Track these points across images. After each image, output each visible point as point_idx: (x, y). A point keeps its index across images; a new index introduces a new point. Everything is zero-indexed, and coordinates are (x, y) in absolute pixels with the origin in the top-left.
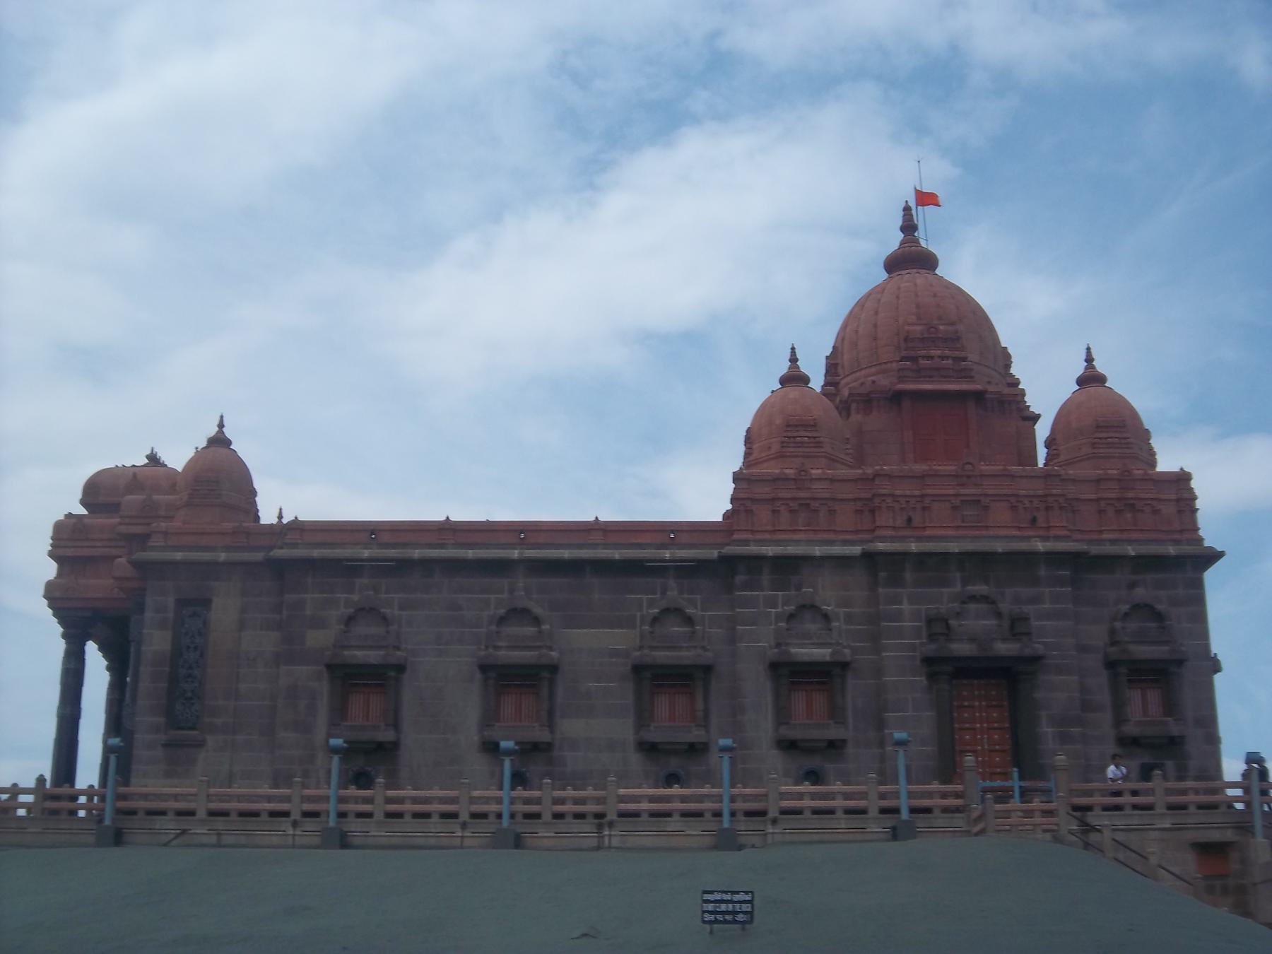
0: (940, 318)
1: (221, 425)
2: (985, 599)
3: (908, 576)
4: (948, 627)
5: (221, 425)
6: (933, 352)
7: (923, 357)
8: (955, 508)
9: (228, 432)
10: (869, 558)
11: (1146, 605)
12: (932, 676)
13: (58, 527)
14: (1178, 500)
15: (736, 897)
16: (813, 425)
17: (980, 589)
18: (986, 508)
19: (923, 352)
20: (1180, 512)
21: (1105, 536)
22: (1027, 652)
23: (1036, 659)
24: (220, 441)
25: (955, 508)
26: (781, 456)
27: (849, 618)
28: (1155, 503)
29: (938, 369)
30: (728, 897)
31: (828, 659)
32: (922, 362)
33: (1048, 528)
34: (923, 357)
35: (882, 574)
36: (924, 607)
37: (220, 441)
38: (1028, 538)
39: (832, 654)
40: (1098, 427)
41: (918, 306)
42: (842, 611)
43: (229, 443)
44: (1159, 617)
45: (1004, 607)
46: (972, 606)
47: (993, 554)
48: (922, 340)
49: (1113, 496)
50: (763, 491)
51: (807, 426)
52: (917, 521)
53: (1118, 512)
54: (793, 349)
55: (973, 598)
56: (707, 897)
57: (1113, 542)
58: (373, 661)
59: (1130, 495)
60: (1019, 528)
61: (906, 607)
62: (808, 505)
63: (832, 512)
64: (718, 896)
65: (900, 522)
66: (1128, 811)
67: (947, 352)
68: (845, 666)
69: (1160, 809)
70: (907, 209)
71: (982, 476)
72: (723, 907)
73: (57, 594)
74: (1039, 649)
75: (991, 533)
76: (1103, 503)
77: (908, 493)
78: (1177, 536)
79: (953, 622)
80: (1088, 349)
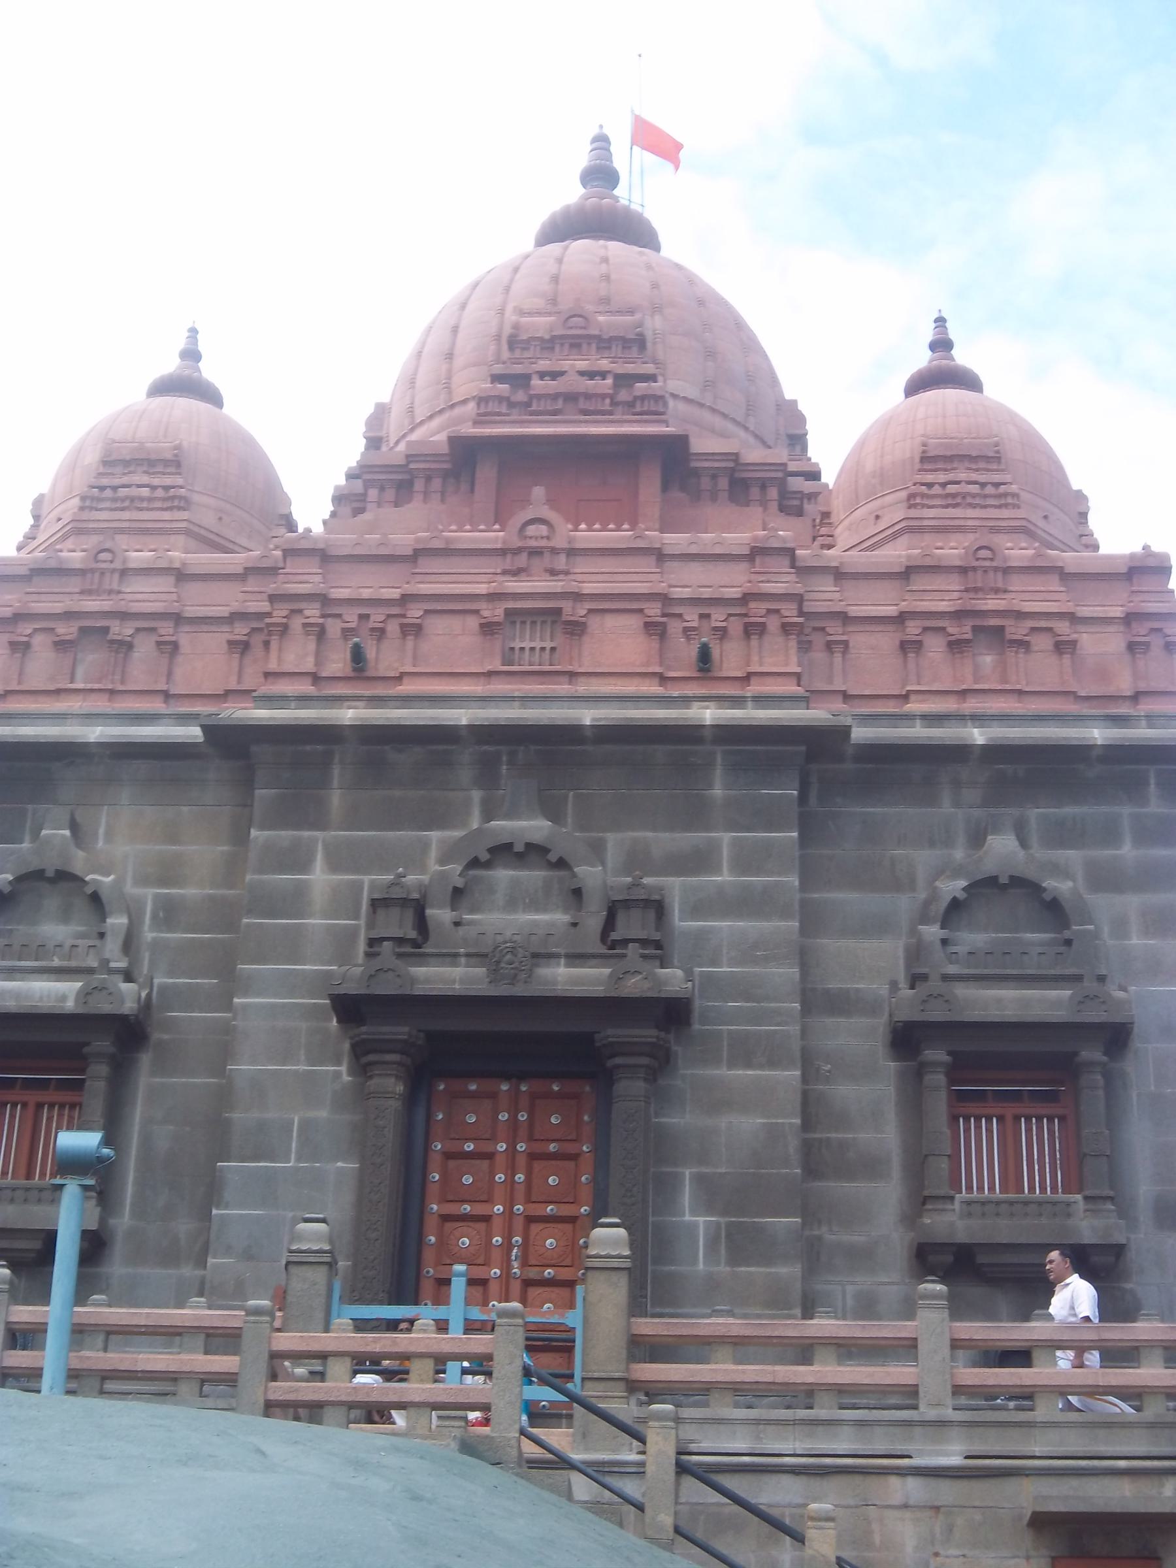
0: (606, 300)
2: (533, 853)
3: (336, 799)
4: (422, 923)
6: (566, 365)
7: (542, 375)
8: (488, 629)
10: (232, 744)
11: (1017, 882)
12: (363, 1057)
14: (1129, 619)
16: (175, 463)
17: (532, 827)
18: (576, 629)
19: (544, 365)
20: (1132, 647)
21: (913, 707)
22: (634, 987)
23: (673, 1013)
25: (488, 629)
26: (78, 529)
27: (169, 914)
28: (1062, 627)
29: (571, 398)
31: (70, 1006)
32: (536, 382)
33: (747, 678)
34: (542, 375)
35: (262, 794)
36: (366, 879)
38: (686, 701)
39: (85, 995)
40: (928, 460)
41: (555, 279)
42: (149, 894)
44: (1054, 911)
45: (589, 874)
46: (503, 875)
47: (570, 734)
48: (549, 344)
51: (151, 463)
52: (386, 658)
53: (956, 646)
55: (503, 852)
57: (932, 719)
59: (992, 604)
60: (663, 679)
61: (320, 878)
62: (106, 630)
63: (171, 649)
65: (338, 663)
67: (604, 364)
68: (129, 1034)
70: (602, 142)
71: (572, 552)
74: (672, 979)
75: (582, 688)
76: (913, 628)
77: (366, 593)
78: (1123, 709)
79: (440, 915)
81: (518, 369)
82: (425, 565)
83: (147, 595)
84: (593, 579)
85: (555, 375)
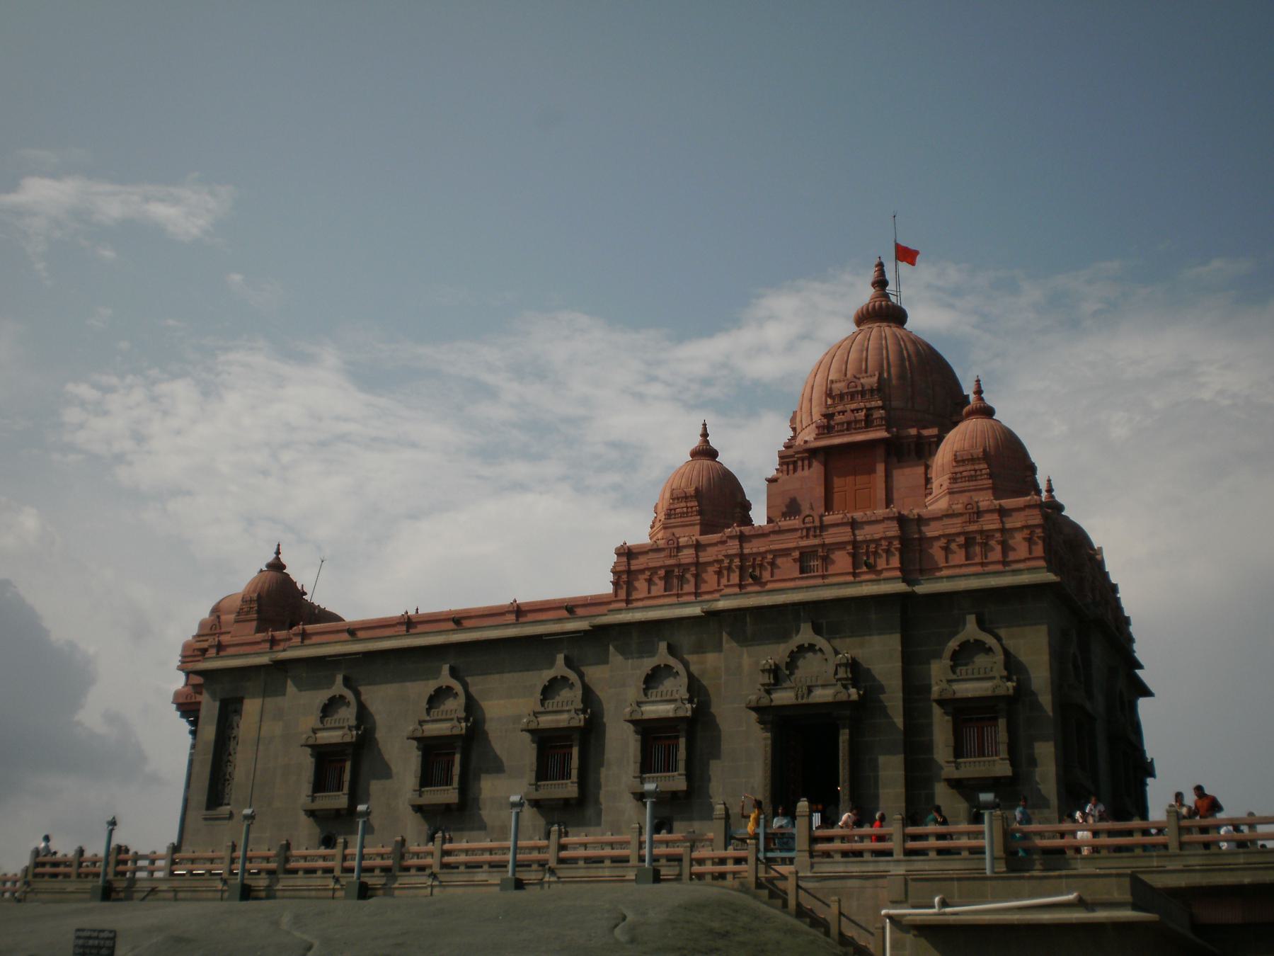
1: (278, 553)
5: (278, 553)
9: (284, 558)
13: (186, 647)
15: (102, 935)
24: (277, 566)
29: (849, 423)
30: (95, 934)
37: (277, 566)
43: (284, 567)
49: (953, 531)
50: (636, 564)
54: (705, 425)
56: (81, 934)
57: (949, 578)
58: (562, 725)
64: (87, 934)
66: (867, 857)
69: (899, 855)
72: (91, 942)
73: (181, 701)
77: (755, 550)
80: (978, 381)
81: (831, 410)
82: (773, 537)
83: (687, 556)
84: (830, 537)
85: (843, 412)
